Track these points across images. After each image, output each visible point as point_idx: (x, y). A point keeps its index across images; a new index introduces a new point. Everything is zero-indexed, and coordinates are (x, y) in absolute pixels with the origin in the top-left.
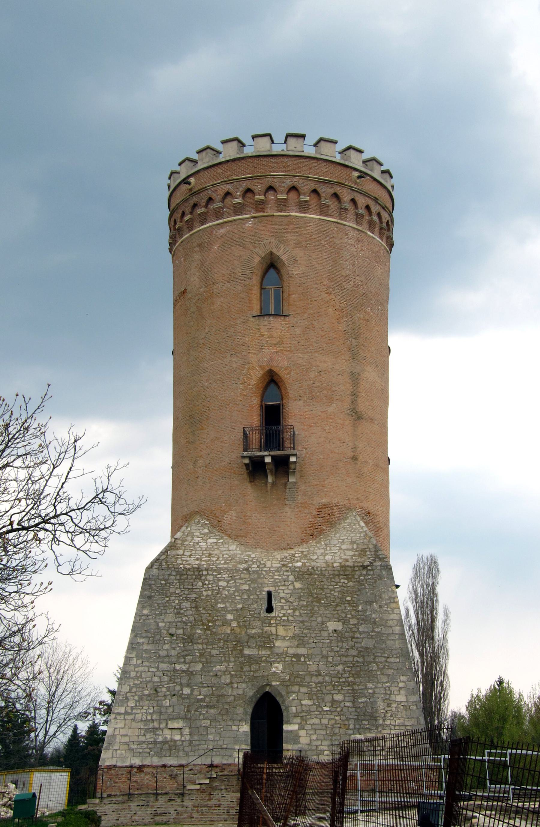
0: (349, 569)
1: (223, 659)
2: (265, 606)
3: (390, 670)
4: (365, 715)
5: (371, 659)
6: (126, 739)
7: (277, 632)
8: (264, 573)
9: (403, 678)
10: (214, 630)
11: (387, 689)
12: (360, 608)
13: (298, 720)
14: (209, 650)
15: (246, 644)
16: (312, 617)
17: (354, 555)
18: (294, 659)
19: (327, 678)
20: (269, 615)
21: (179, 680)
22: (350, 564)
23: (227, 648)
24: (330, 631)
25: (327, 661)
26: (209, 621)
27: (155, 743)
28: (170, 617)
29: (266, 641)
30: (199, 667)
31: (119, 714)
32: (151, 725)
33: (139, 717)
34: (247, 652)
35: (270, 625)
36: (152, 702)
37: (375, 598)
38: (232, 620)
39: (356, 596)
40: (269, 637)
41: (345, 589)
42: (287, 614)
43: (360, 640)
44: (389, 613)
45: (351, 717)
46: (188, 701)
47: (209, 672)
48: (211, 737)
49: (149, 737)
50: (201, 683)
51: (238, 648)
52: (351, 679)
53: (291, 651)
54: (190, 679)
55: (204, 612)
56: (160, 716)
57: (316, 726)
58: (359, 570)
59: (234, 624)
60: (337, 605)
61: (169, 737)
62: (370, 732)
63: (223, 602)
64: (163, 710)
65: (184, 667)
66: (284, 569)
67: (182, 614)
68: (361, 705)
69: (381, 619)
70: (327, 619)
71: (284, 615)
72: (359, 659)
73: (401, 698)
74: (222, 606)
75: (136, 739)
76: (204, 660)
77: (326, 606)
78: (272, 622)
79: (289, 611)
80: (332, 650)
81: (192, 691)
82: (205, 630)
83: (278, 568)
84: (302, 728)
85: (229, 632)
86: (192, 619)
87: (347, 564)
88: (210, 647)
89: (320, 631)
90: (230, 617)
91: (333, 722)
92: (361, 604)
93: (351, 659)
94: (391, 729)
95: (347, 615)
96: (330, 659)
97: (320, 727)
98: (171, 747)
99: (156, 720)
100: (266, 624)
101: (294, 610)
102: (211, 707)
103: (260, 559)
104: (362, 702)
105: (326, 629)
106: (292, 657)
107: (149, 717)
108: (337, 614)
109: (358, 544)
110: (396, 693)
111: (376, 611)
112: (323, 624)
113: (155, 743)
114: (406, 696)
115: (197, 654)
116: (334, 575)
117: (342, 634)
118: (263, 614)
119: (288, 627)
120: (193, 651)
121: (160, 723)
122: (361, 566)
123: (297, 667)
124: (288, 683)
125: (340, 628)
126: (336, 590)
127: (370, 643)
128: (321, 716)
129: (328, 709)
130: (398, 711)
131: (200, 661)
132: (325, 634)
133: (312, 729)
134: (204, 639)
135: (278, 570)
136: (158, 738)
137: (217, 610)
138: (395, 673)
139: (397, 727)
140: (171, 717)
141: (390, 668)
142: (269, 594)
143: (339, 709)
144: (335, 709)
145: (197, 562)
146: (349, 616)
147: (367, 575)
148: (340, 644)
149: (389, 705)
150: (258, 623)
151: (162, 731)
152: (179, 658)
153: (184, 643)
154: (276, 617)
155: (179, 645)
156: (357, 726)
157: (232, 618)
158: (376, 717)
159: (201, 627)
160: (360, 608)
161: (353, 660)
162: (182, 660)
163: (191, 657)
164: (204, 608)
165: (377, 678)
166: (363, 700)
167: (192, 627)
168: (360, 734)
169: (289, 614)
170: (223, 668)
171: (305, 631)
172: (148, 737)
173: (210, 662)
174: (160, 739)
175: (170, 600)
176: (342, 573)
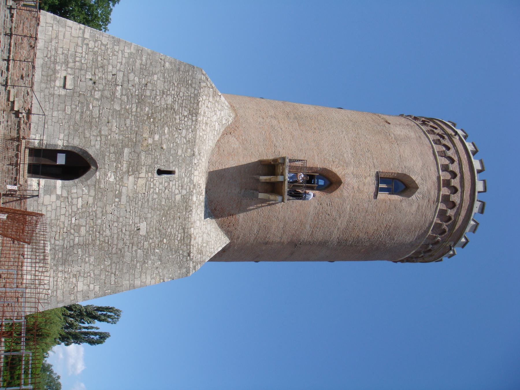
0: (189, 241)
1: (122, 129)
2: (163, 168)
3: (104, 276)
4: (66, 255)
5: (115, 259)
6: (61, 37)
7: (140, 178)
8: (190, 169)
9: (97, 288)
10: (147, 123)
11: (89, 274)
12: (157, 251)
13: (65, 194)
14: (130, 117)
15: (133, 150)
16: (152, 209)
17: (198, 245)
18: (117, 192)
19: (99, 221)
20: (156, 172)
21: (107, 89)
22: (193, 242)
23: (131, 134)
24: (139, 225)
25: (114, 222)
26: (154, 119)
27: (55, 63)
28: (160, 85)
30: (117, 107)
32: (71, 60)
34: (126, 150)
35: (147, 172)
36: (91, 63)
37: (165, 263)
38: (154, 139)
39: (166, 247)
40: (137, 171)
41: (173, 238)
42: (155, 187)
43: (130, 249)
44: (151, 275)
45: (66, 242)
46: (89, 95)
47: (112, 116)
49: (61, 58)
50: (103, 108)
51: (130, 143)
54: (107, 98)
55: (163, 115)
56: (78, 69)
57: (59, 210)
58: (187, 249)
59: (150, 141)
60: (160, 231)
61: (59, 75)
62: (52, 259)
63: (169, 133)
64: (83, 72)
67: (163, 96)
68: (75, 251)
69: (147, 269)
70: (149, 223)
71: (155, 185)
72: (114, 249)
73: (81, 286)
75: (60, 45)
76: (123, 112)
77: (159, 222)
78: (150, 174)
79: (157, 189)
81: (97, 100)
82: (148, 115)
83: (193, 181)
84: (58, 197)
85: (144, 136)
86: (158, 104)
87: (192, 239)
88: (133, 119)
89: (140, 216)
90: (157, 137)
91: (62, 226)
92: (160, 251)
94: (54, 277)
95: (152, 239)
97: (58, 214)
99: (75, 65)
100: (149, 168)
101: (158, 194)
103: (200, 166)
104: (78, 252)
105: (141, 221)
106: (119, 191)
107: (78, 59)
108: (153, 231)
109: (206, 247)
110: (85, 281)
111: (154, 264)
112: (145, 219)
113: (55, 63)
114: (82, 291)
115: (128, 107)
116: (184, 229)
117: (136, 235)
119: (144, 188)
120: (131, 103)
121: (71, 68)
122: (190, 251)
124: (97, 187)
125: (141, 233)
126: (172, 230)
128: (67, 215)
129: (73, 222)
130: (69, 284)
131: (122, 108)
132: (137, 220)
133: (57, 207)
134: (140, 114)
135: (191, 181)
136: (58, 66)
137: (163, 127)
138: (102, 281)
139: (55, 283)
140: (76, 79)
141: (106, 276)
143: (72, 231)
144: (73, 227)
146: (151, 241)
147: (184, 256)
148: (128, 233)
149: (75, 276)
150: (150, 162)
151: (65, 70)
152: (126, 90)
153: (138, 95)
154: (153, 178)
155: (137, 91)
156: (57, 248)
157: (155, 139)
158: (65, 264)
159: (150, 112)
160: (157, 251)
161: (113, 245)
162: (124, 93)
163: (126, 101)
164: (165, 115)
165: (98, 265)
166: (80, 253)
167: (151, 105)
168: (50, 250)
169: (155, 189)
170: (114, 129)
171: (140, 203)
172: (61, 56)
173: (120, 118)
175: (175, 86)
176: (186, 235)
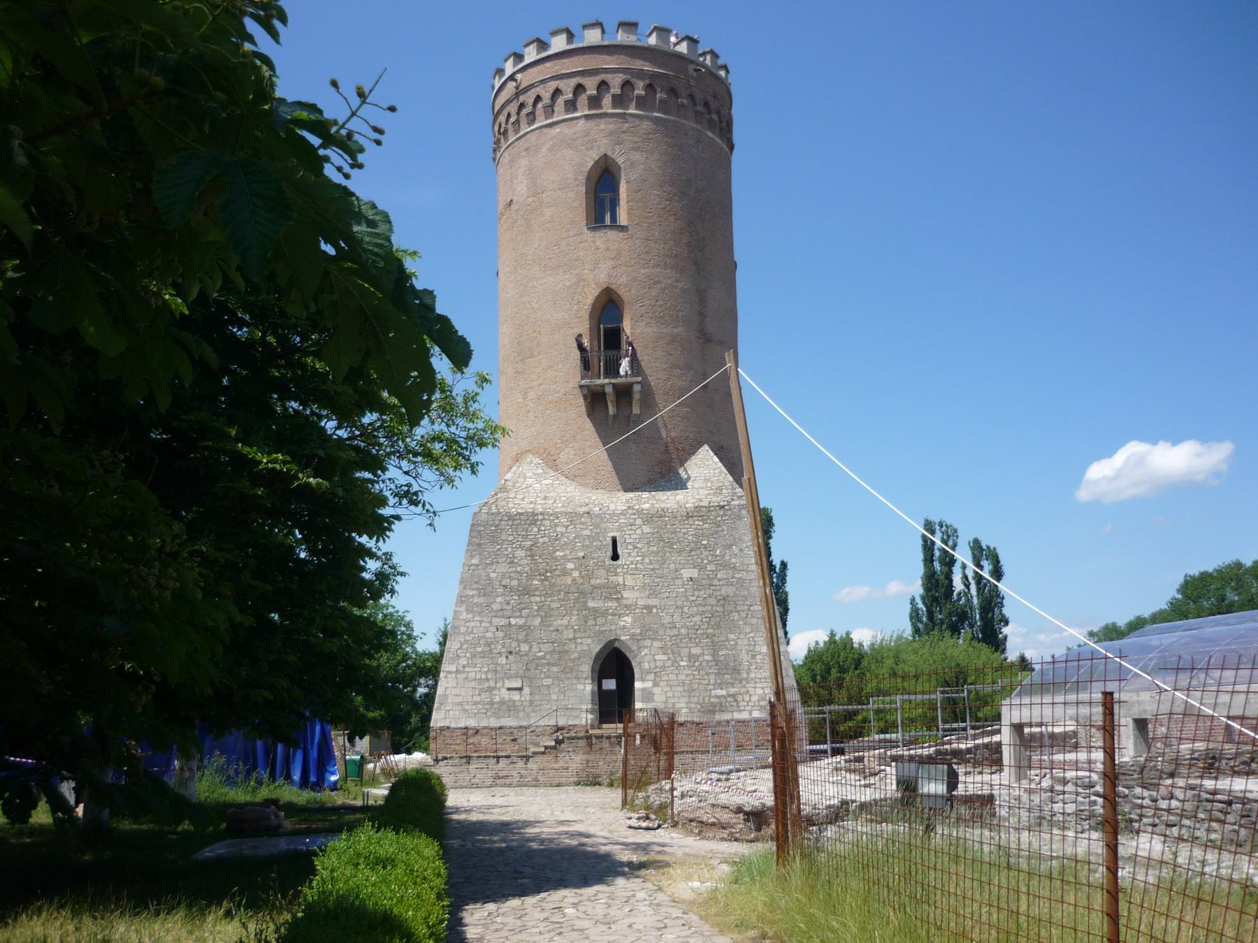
27: (492, 703)
29: (613, 592)
30: (538, 620)
31: (450, 672)
32: (487, 685)
33: (472, 675)
34: (591, 604)
35: (616, 574)
48: (554, 697)
52: (710, 631)
53: (641, 602)
64: (499, 668)
65: (521, 622)
80: (688, 600)
86: (527, 569)
90: (570, 566)
93: (709, 608)
96: (686, 610)
98: (509, 708)
102: (553, 665)
113: (492, 703)
118: (609, 562)
123: (648, 619)
127: (730, 591)
142: (614, 541)
170: (565, 622)
174: (497, 699)
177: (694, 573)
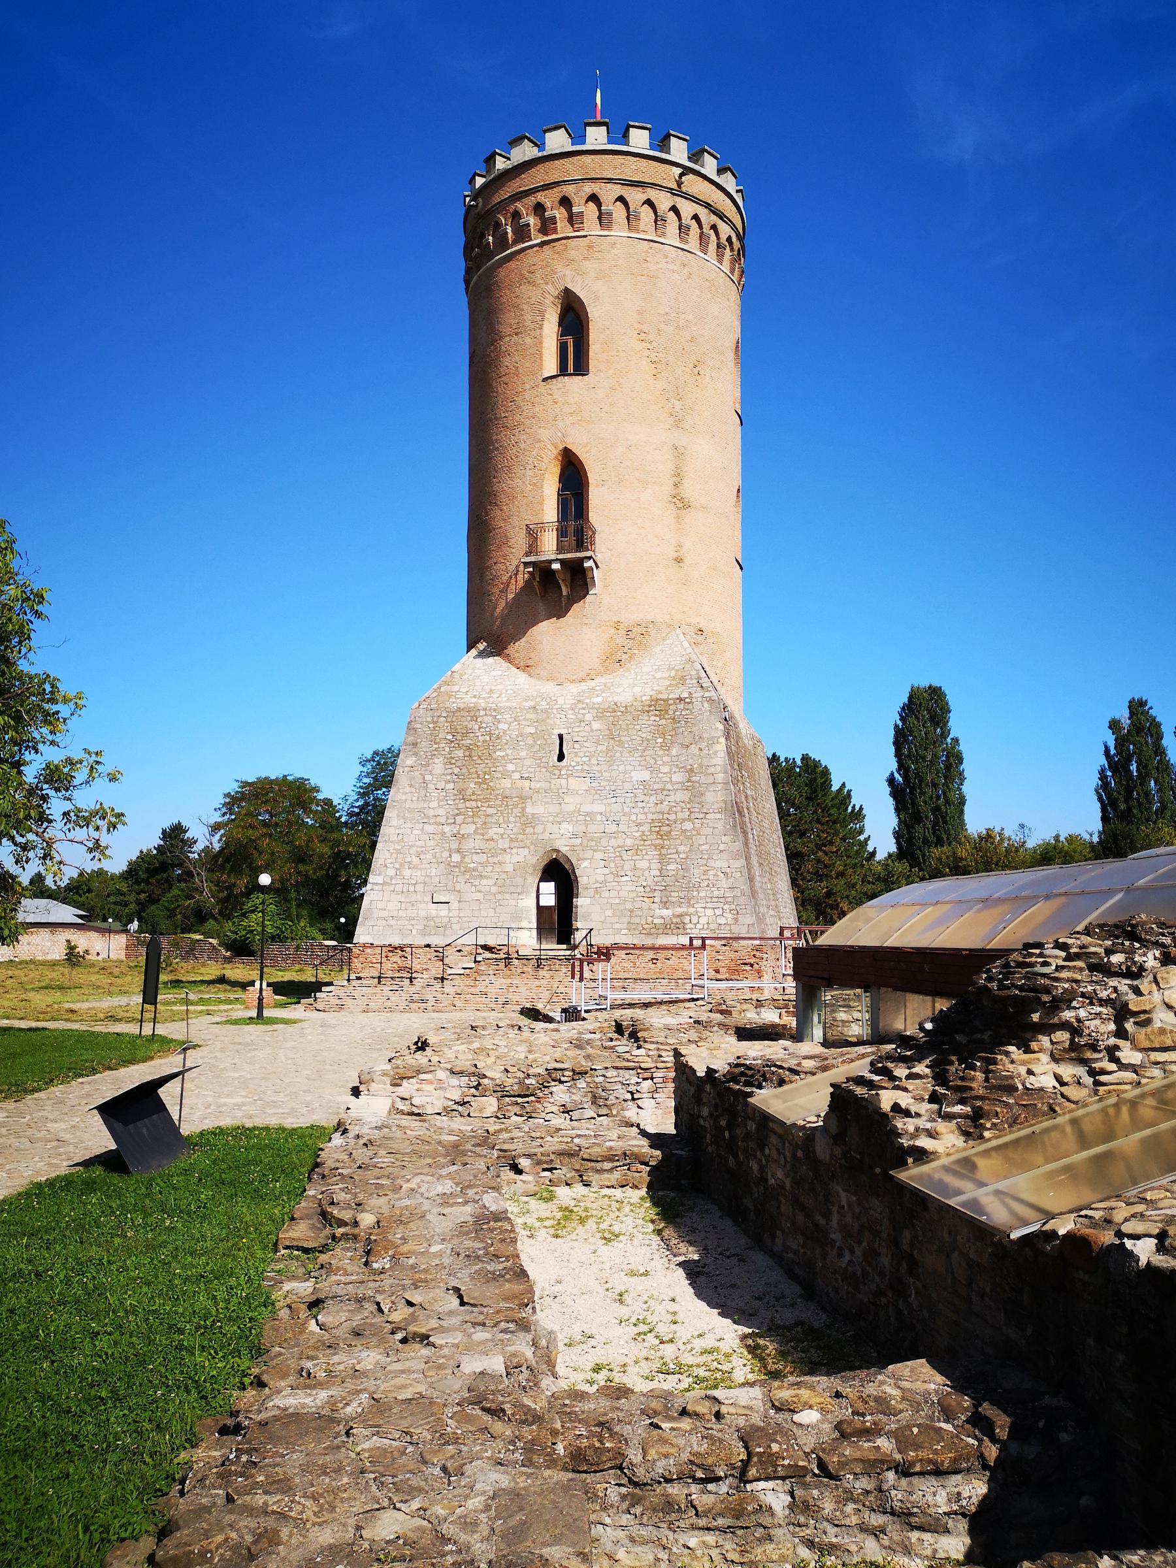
26: (485, 773)
66: (580, 706)
74: (502, 754)
81: (463, 857)
145: (474, 700)
177: (646, 775)
